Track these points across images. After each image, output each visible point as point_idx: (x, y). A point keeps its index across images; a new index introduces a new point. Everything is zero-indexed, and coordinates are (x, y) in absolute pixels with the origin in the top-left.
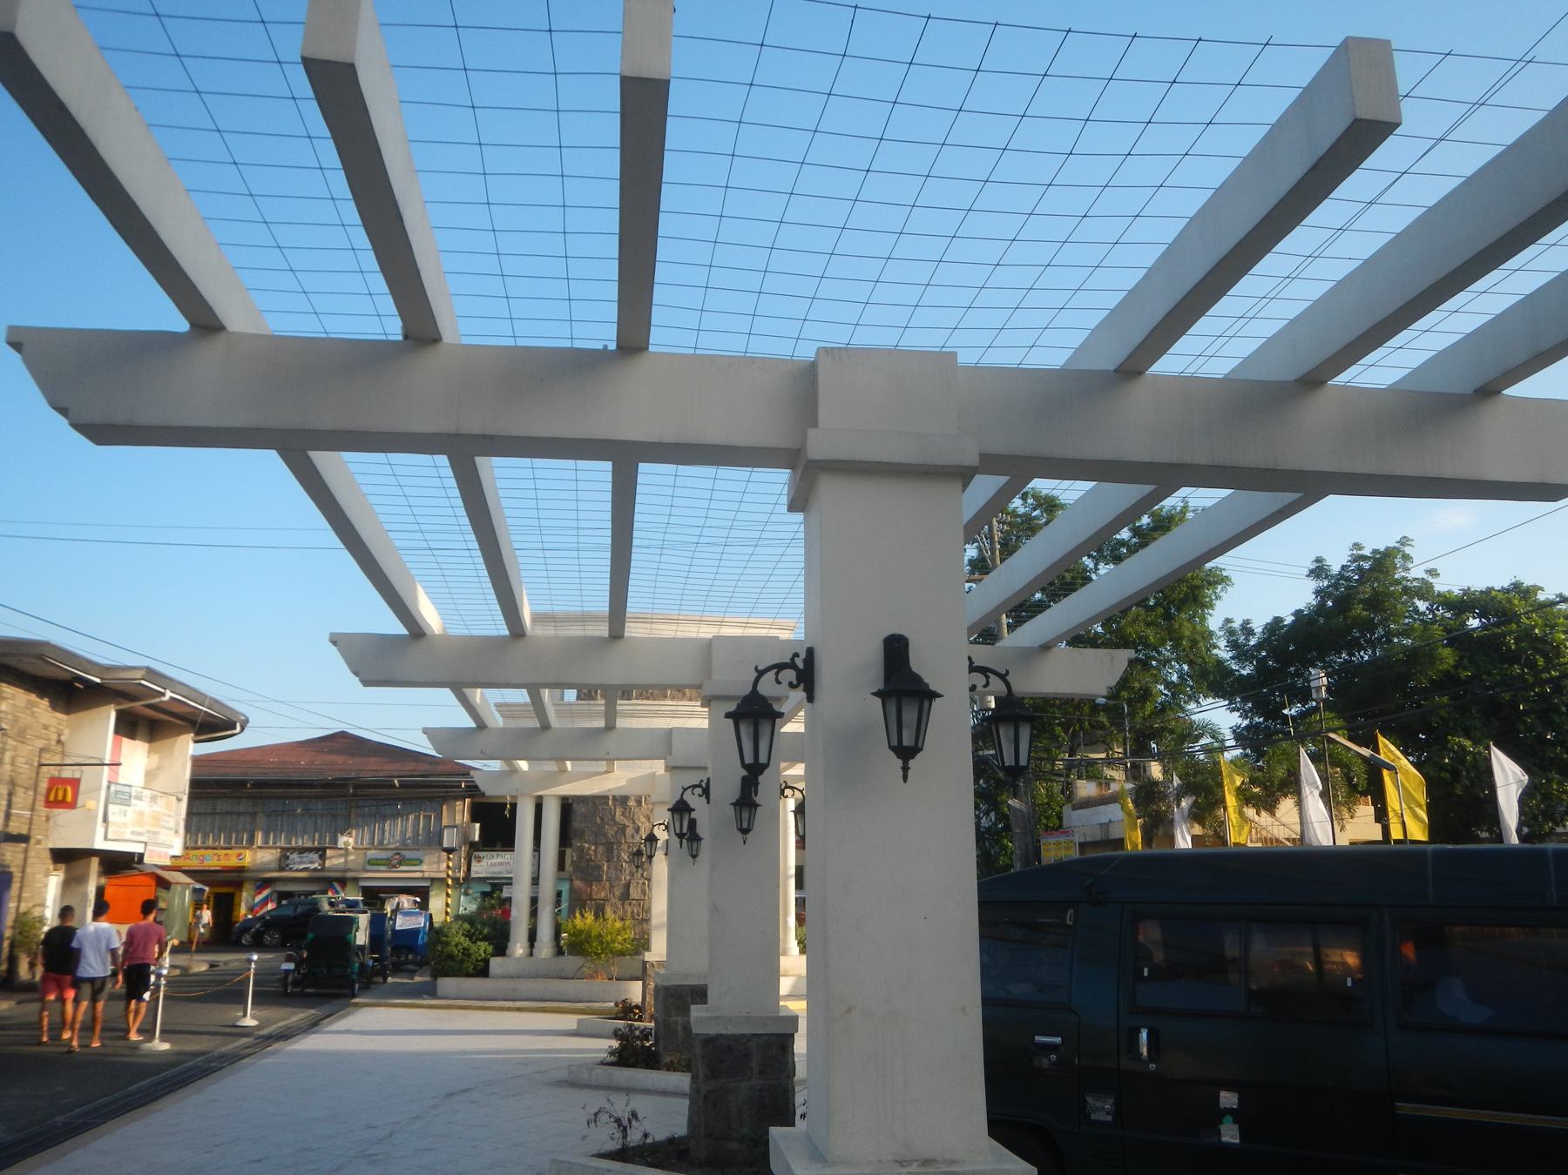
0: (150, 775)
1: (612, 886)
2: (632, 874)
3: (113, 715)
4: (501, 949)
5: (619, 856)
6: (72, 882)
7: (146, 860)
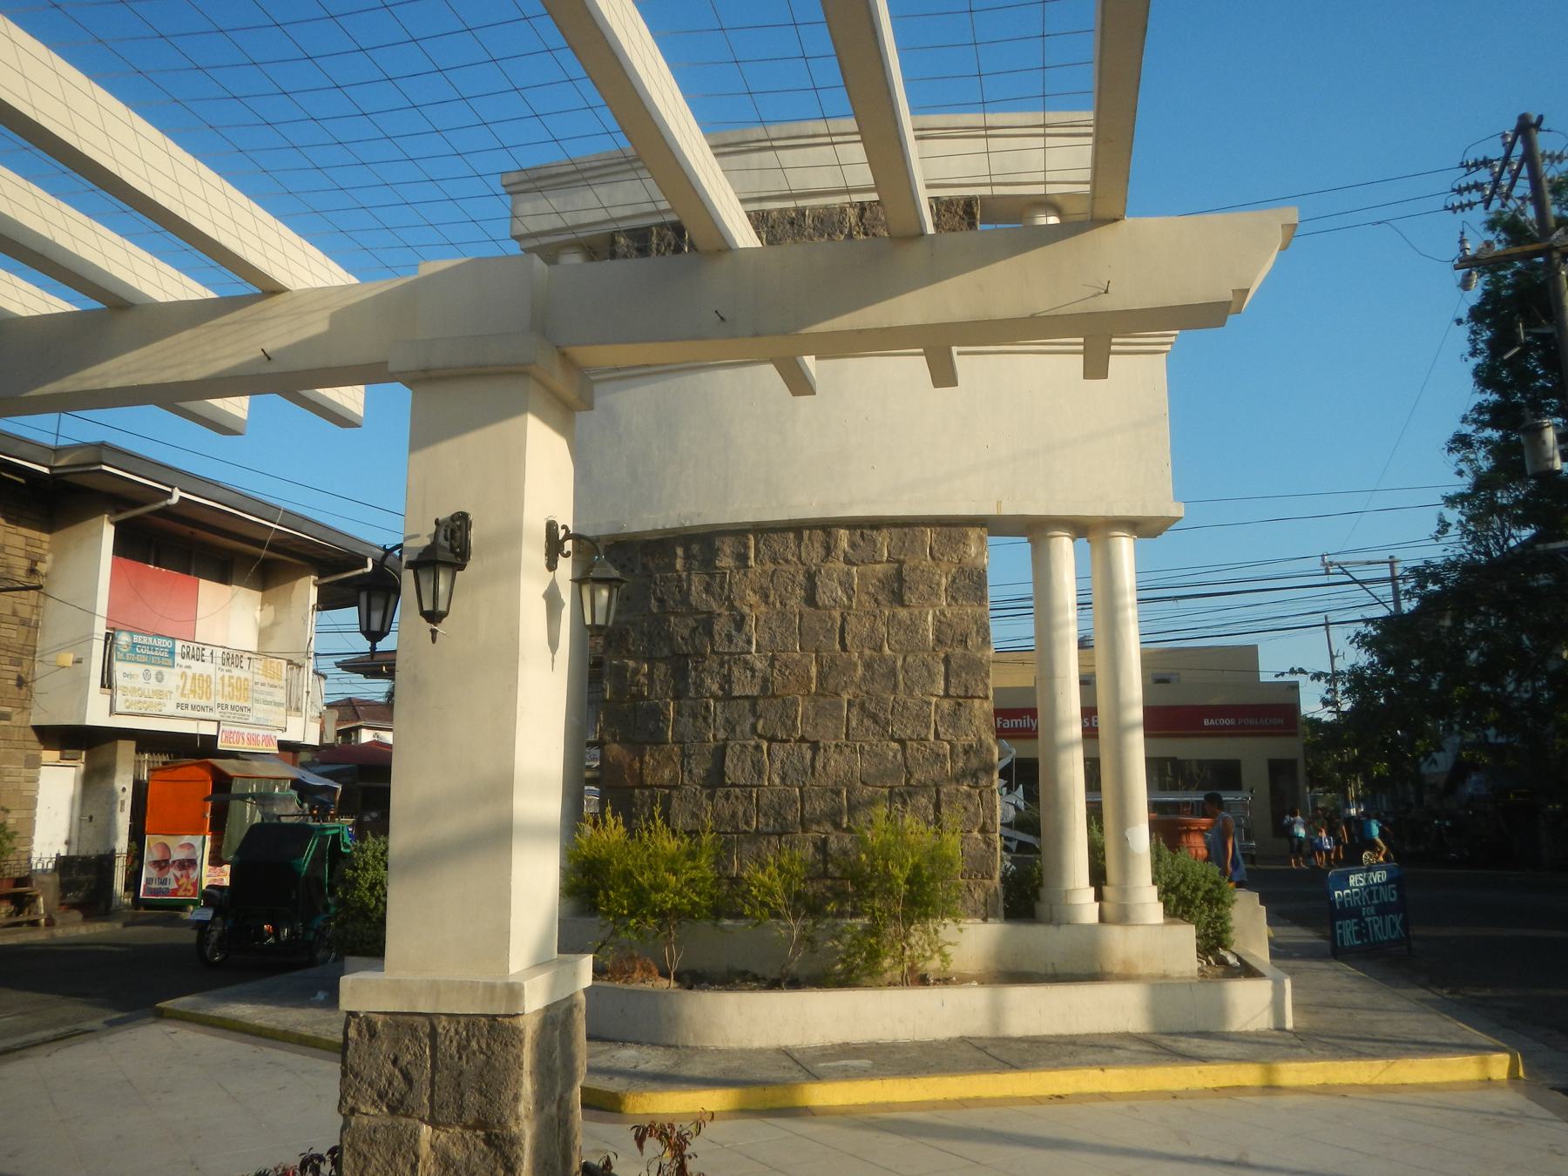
0: (264, 634)
1: (685, 755)
2: (730, 726)
3: (109, 532)
5: (699, 685)
6: (95, 779)
7: (222, 745)
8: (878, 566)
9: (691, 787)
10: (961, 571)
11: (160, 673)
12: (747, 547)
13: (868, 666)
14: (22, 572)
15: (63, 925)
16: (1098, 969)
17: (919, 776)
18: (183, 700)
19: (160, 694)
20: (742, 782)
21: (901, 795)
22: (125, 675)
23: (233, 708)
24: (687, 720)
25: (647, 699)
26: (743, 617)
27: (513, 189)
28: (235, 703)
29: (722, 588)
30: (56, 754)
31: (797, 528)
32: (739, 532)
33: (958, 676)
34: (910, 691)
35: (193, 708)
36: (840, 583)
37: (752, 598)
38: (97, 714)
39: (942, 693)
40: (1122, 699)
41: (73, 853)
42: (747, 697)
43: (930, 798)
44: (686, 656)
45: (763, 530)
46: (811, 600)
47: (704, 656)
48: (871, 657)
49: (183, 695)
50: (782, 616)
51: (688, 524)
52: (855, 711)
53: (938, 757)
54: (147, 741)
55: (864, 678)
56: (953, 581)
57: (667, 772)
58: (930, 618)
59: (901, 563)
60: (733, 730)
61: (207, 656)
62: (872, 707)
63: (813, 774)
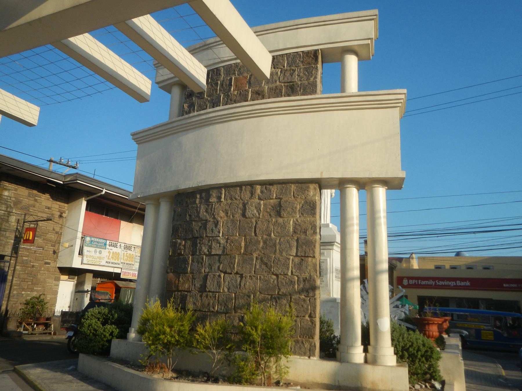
1: (193, 278)
3: (84, 204)
4: (123, 335)
5: (200, 250)
7: (122, 276)
8: (272, 201)
9: (195, 292)
10: (306, 202)
11: (101, 251)
12: (221, 194)
13: (265, 242)
14: (57, 216)
15: (59, 335)
16: (360, 385)
17: (283, 290)
18: (109, 261)
19: (100, 258)
20: (213, 290)
21: (275, 298)
22: (88, 251)
23: (127, 264)
24: (195, 264)
25: (182, 255)
26: (218, 222)
27: (156, 66)
28: (128, 262)
29: (211, 210)
30: (67, 277)
31: (240, 185)
32: (219, 187)
33: (302, 247)
34: (281, 253)
35: (112, 263)
36: (256, 208)
37: (222, 214)
38: (77, 264)
39: (294, 254)
40: (377, 259)
41: (71, 311)
42: (217, 255)
43: (288, 300)
44: (197, 238)
45: (227, 186)
46: (244, 215)
47: (203, 238)
48: (266, 239)
49: (109, 259)
50: (233, 221)
51: (200, 185)
52: (259, 261)
53: (292, 283)
54: (97, 274)
55: (263, 248)
56: (302, 207)
57: (187, 285)
58: (291, 222)
59: (281, 199)
60: (211, 268)
61: (118, 246)
62: (265, 260)
63: (240, 288)
